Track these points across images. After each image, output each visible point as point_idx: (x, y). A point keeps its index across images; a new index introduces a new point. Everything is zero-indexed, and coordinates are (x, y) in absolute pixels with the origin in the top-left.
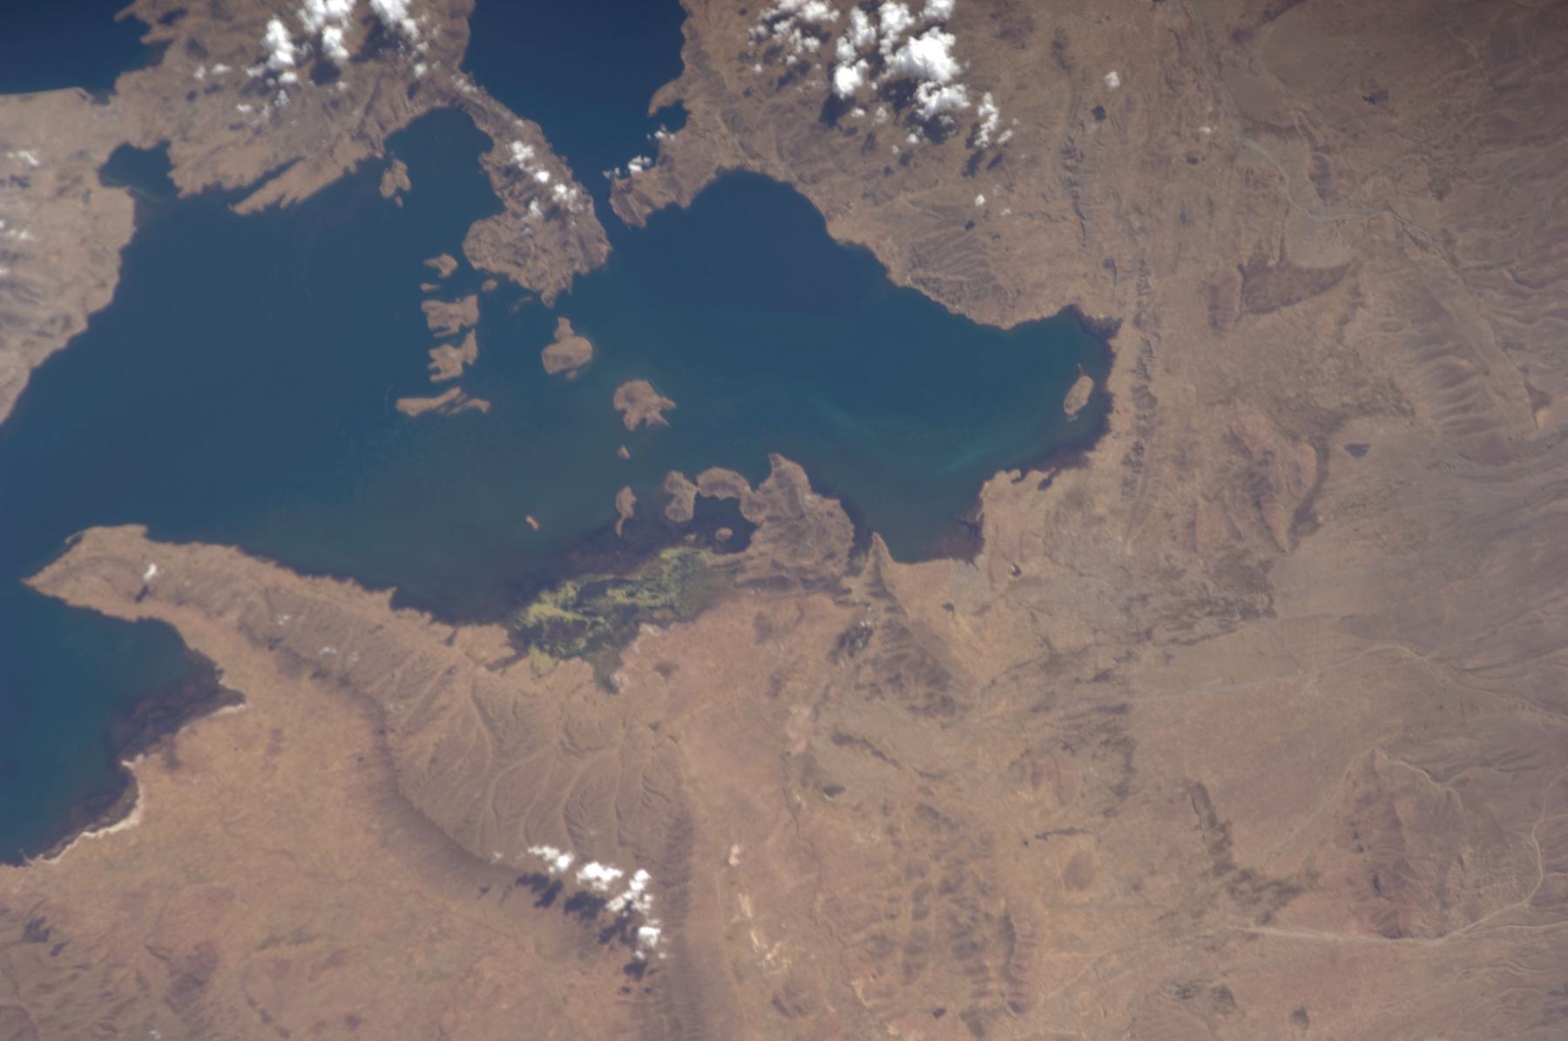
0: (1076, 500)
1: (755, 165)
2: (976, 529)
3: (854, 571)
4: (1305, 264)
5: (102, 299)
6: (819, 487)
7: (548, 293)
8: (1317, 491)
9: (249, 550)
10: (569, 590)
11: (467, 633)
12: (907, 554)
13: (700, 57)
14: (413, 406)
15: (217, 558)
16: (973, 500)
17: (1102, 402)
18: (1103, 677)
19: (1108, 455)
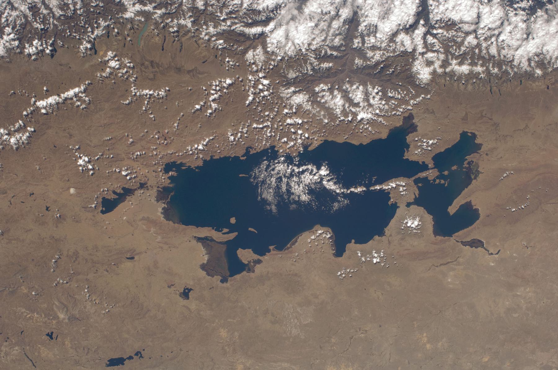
0: (480, 136)
1: (432, 157)
2: (480, 144)
3: (480, 153)
4: (464, 115)
5: (423, 208)
6: (470, 155)
7: (439, 174)
8: (489, 118)
9: (456, 198)
10: (472, 175)
11: (472, 183)
12: (480, 149)
13: (418, 160)
14: (446, 185)
15: (455, 201)
16: (477, 144)
17: (471, 133)
18: (499, 136)
19: (476, 133)
